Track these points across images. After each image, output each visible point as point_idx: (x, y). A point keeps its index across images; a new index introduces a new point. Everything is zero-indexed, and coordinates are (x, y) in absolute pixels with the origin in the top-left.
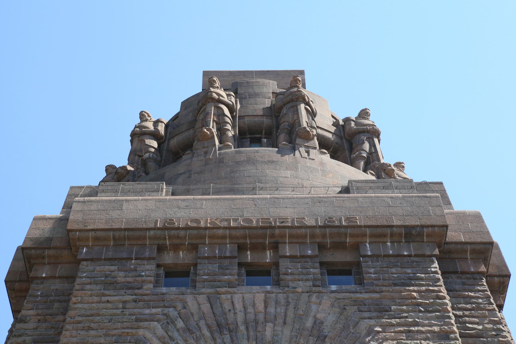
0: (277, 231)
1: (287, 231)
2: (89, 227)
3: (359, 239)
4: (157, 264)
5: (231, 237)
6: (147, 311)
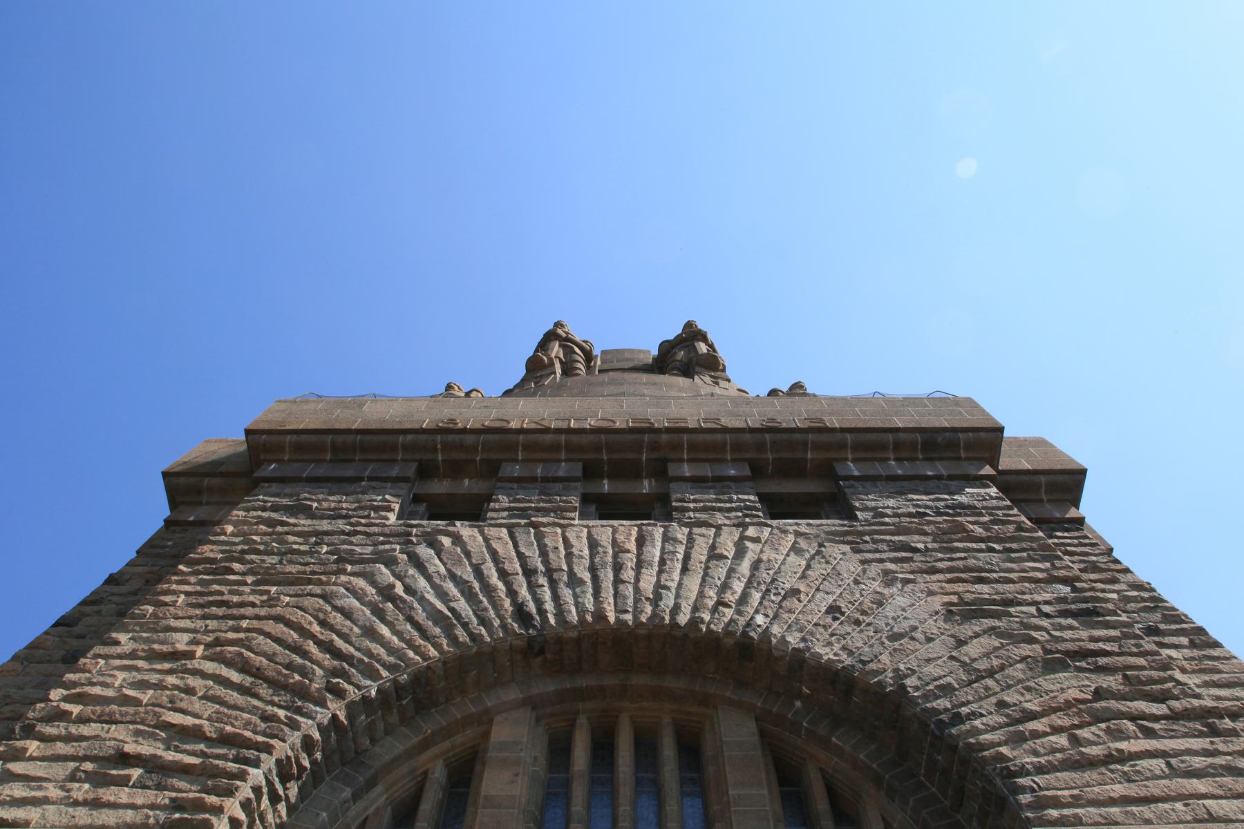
0: (665, 437)
1: (685, 437)
2: (287, 427)
3: (832, 455)
4: (414, 495)
5: (570, 448)
6: (369, 549)
